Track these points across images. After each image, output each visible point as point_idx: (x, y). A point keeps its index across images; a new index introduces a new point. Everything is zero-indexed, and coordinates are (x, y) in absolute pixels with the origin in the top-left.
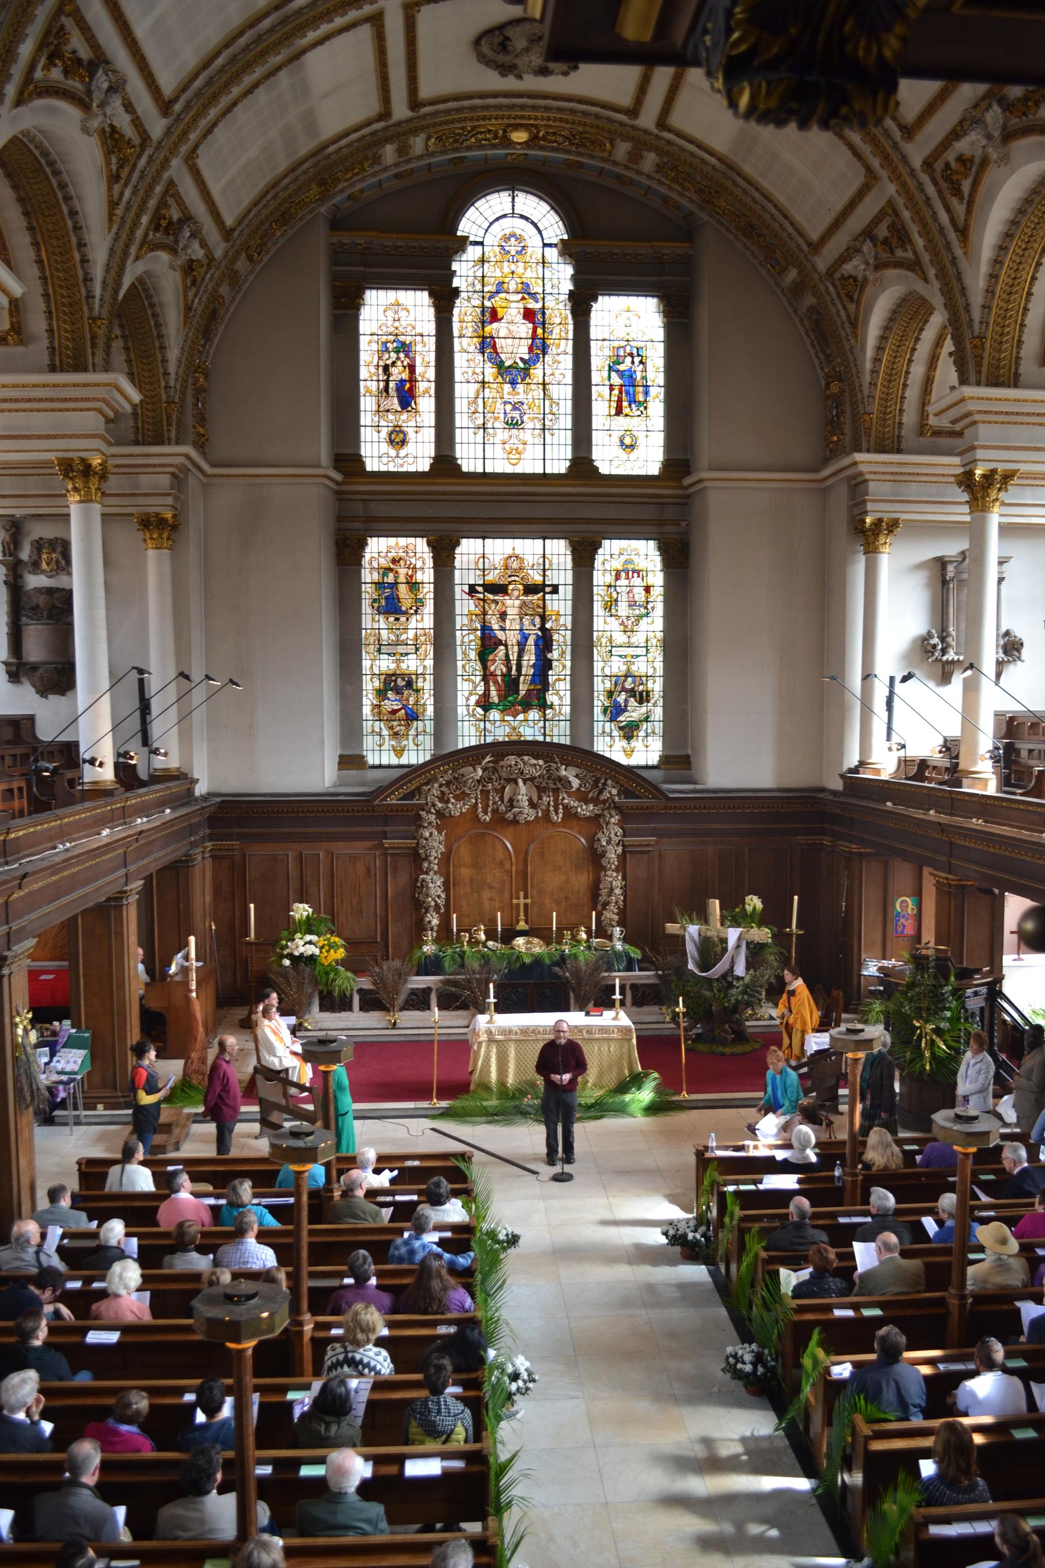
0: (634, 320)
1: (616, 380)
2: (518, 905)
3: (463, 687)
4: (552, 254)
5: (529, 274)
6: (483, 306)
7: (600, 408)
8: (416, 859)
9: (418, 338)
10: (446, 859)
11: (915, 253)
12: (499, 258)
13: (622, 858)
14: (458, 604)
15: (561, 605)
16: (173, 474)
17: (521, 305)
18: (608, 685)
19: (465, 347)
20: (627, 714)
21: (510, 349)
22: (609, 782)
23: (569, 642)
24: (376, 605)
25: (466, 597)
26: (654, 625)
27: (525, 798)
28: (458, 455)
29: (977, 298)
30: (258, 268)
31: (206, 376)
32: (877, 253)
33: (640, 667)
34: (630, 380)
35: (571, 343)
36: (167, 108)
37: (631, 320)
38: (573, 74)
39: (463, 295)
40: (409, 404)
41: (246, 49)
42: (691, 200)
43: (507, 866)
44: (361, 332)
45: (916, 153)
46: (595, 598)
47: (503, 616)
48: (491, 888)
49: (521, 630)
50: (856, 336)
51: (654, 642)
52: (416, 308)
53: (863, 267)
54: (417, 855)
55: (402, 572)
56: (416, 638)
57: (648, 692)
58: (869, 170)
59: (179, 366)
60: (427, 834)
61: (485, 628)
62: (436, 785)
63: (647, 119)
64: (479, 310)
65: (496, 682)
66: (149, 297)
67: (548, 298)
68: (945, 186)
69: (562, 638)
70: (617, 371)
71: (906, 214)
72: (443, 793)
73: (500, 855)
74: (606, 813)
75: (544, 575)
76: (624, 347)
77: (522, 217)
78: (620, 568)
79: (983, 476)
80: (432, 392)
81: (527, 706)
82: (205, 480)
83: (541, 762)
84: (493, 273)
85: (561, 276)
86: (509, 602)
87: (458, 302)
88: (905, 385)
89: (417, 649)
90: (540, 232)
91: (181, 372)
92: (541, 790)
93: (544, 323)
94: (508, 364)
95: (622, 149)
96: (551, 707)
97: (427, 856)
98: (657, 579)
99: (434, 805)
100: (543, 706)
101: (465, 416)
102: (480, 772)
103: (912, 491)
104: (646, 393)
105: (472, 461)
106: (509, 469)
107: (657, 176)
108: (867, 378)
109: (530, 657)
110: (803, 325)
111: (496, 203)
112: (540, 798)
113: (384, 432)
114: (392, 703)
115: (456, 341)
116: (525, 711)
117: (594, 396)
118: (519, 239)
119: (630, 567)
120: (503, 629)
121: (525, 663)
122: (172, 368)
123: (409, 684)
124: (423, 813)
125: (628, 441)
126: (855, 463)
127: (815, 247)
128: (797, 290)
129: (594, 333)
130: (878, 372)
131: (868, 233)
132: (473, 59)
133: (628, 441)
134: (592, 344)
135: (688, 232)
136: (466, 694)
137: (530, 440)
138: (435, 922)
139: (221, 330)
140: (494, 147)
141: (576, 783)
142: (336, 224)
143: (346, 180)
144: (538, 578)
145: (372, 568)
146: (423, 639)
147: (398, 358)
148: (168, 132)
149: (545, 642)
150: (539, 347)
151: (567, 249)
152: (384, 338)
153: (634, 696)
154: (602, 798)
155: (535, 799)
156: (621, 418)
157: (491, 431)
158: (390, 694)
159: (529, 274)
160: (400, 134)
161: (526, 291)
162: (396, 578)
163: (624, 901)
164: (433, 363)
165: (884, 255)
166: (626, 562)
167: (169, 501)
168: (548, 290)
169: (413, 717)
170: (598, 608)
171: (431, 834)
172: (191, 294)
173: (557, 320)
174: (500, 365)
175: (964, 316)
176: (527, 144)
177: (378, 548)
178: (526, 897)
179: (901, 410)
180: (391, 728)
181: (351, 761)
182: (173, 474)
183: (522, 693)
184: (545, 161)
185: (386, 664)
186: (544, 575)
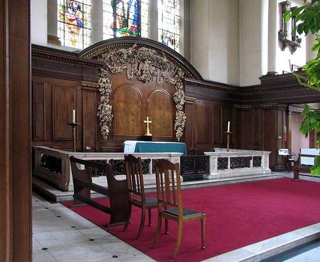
57: (175, 40)
109: (133, 10)
114: (70, 15)
123: (79, 8)
183: (129, 27)
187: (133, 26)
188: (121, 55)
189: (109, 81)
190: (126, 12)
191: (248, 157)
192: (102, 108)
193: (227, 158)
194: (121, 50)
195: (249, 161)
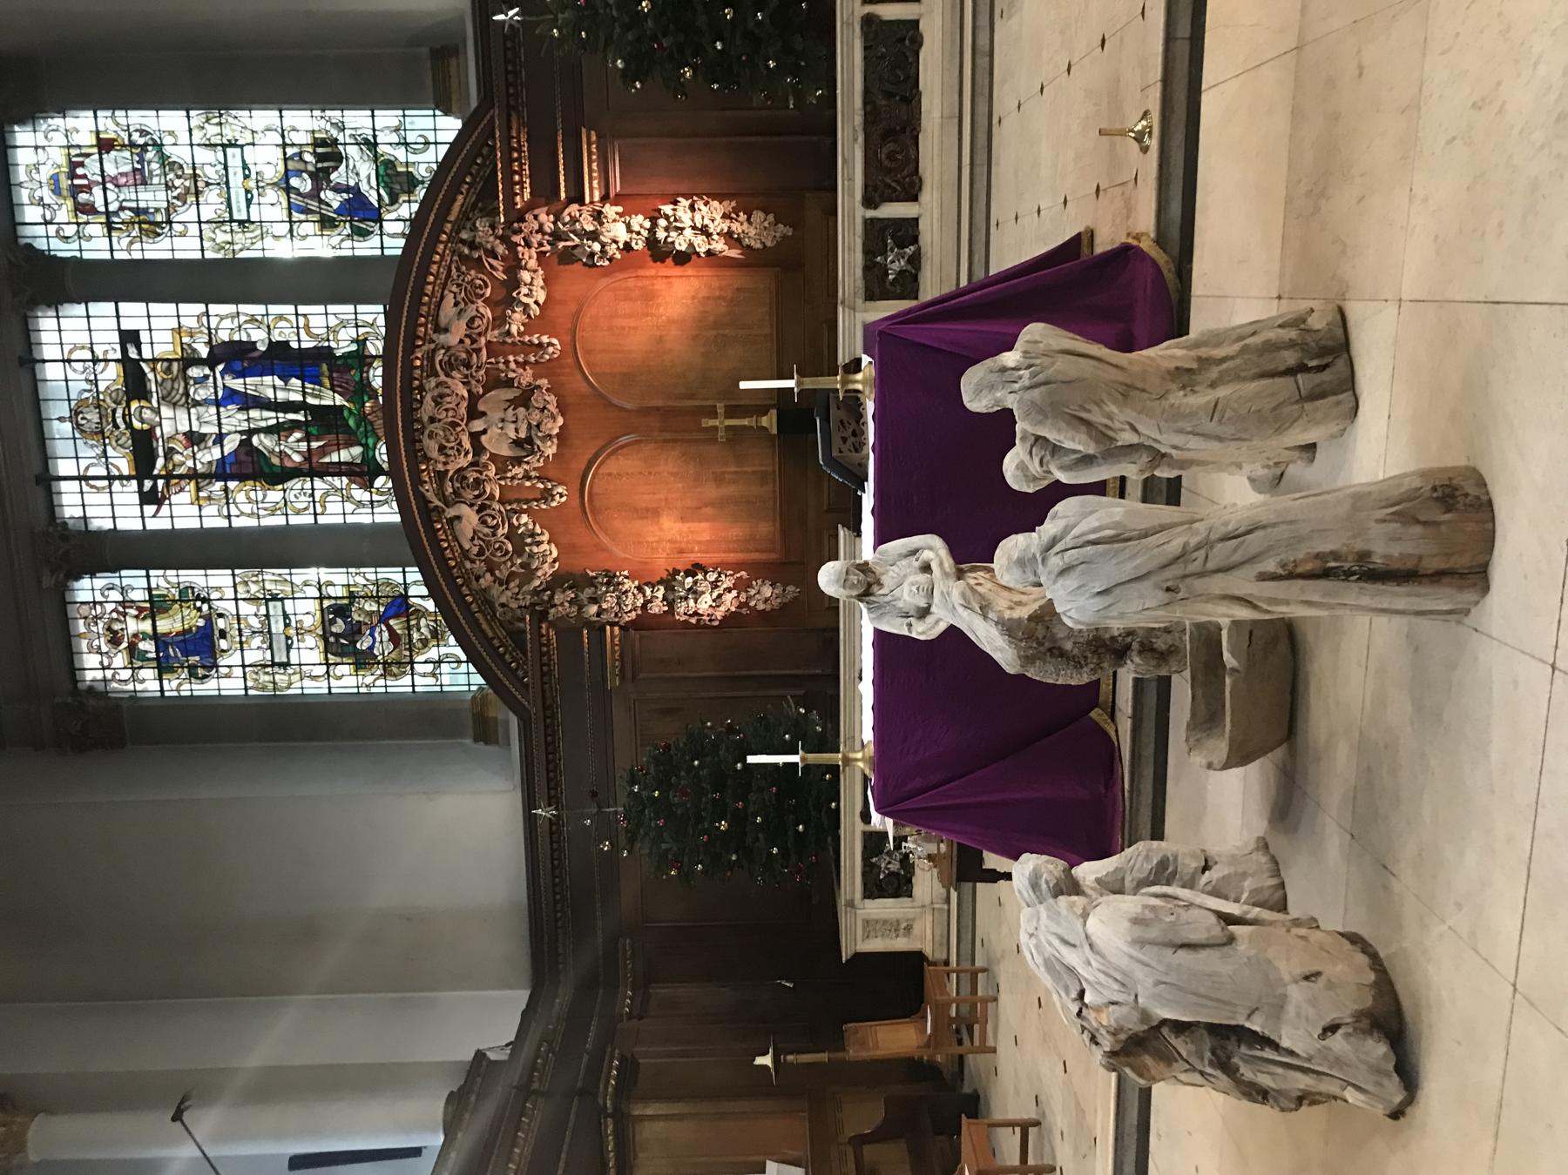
2: (728, 428)
3: (334, 514)
14: (180, 524)
15: (162, 326)
18: (309, 228)
20: (364, 187)
22: (464, 235)
24: (200, 672)
25: (165, 510)
33: (267, 160)
46: (137, 255)
47: (194, 439)
51: (212, 130)
55: (133, 626)
56: (253, 599)
57: (317, 143)
61: (223, 471)
65: (323, 451)
78: (70, 203)
89: (275, 598)
96: (361, 342)
98: (82, 126)
99: (536, 592)
100: (360, 358)
109: (266, 385)
112: (509, 383)
119: (65, 183)
120: (220, 439)
121: (281, 396)
123: (341, 611)
136: (349, 507)
138: (767, 591)
144: (111, 374)
145: (134, 678)
146: (254, 588)
149: (235, 356)
153: (327, 172)
155: (510, 394)
158: (363, 644)
162: (145, 636)
166: (57, 191)
169: (400, 605)
170: (157, 250)
178: (714, 415)
180: (425, 643)
183: (339, 400)
185: (309, 652)
186: (106, 361)
187: (327, 382)
189: (589, 591)
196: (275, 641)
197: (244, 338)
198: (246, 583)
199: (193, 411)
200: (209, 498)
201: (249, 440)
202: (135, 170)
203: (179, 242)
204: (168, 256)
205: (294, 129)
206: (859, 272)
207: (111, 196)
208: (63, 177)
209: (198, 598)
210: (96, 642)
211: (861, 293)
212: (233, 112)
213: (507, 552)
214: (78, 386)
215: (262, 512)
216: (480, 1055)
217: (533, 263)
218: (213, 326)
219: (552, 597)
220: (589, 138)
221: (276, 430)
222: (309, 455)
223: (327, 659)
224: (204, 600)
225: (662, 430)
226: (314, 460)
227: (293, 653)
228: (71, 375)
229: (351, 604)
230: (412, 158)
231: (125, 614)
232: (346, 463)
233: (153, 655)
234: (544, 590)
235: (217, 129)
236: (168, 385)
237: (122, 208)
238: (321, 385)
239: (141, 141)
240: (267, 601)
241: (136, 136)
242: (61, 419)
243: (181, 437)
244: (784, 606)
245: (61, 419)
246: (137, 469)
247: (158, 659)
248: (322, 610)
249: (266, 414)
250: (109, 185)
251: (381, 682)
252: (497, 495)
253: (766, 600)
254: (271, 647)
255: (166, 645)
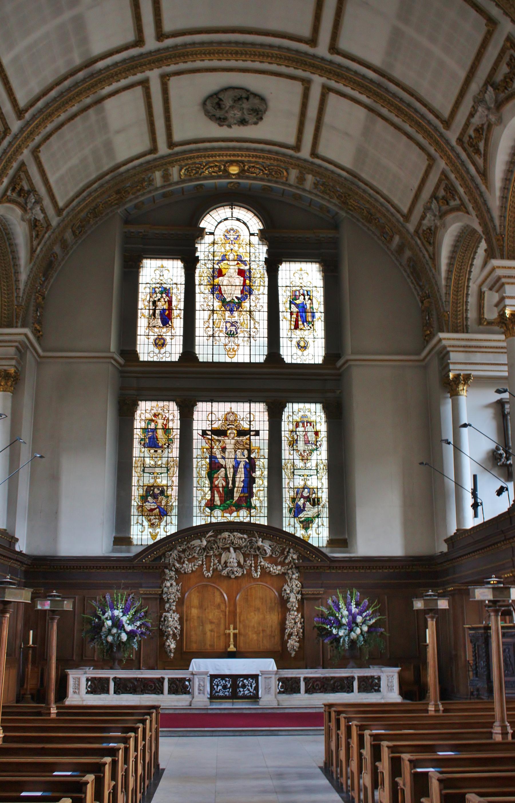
0: (305, 276)
1: (294, 309)
2: (229, 634)
4: (255, 240)
5: (241, 250)
6: (214, 268)
7: (285, 326)
8: (161, 601)
9: (174, 286)
10: (180, 602)
11: (460, 199)
12: (223, 241)
13: (301, 602)
14: (195, 441)
16: (17, 347)
17: (236, 267)
18: (292, 494)
19: (203, 290)
20: (305, 513)
21: (230, 292)
22: (291, 550)
23: (266, 466)
24: (143, 442)
26: (322, 455)
27: (235, 561)
28: (197, 352)
29: (496, 213)
30: (80, 241)
31: (44, 298)
32: (440, 207)
33: (313, 482)
34: (303, 310)
35: (266, 288)
36: (21, 113)
37: (303, 276)
38: (261, 124)
39: (202, 262)
40: (168, 323)
41: (69, 89)
42: (335, 205)
43: (223, 607)
44: (140, 282)
45: (452, 136)
46: (283, 438)
47: (224, 449)
48: (211, 623)
49: (235, 458)
50: (435, 266)
51: (322, 466)
52: (173, 271)
53: (433, 218)
54: (162, 599)
55: (160, 422)
57: (318, 499)
58: (430, 156)
59: (26, 286)
60: (168, 584)
61: (212, 457)
62: (176, 552)
63: (305, 153)
64: (211, 270)
65: (218, 492)
66: (9, 239)
67: (252, 263)
68: (470, 150)
69: (262, 463)
70: (295, 304)
71: (452, 176)
72: (180, 558)
73: (218, 600)
74: (290, 571)
75: (250, 425)
76: (299, 291)
77: (238, 220)
78: (299, 420)
79: (512, 314)
80: (182, 316)
81: (238, 507)
82: (38, 359)
83: (245, 536)
84: (219, 250)
85: (260, 251)
86: (227, 441)
87: (198, 266)
88: (467, 294)
89: (168, 470)
90: (248, 228)
91: (27, 290)
92: (245, 556)
93: (250, 277)
94: (228, 300)
95: (294, 173)
96: (255, 508)
97: (168, 601)
98: (322, 427)
99: (174, 566)
100: (250, 507)
101: (202, 330)
102: (205, 543)
103: (478, 358)
104: (313, 317)
105: (205, 356)
106: (228, 360)
107: (315, 191)
108: (443, 291)
109: (241, 475)
110: (406, 271)
111: (224, 212)
112: (245, 561)
113: (152, 338)
114: (150, 504)
115: (197, 287)
116: (237, 510)
117: (281, 318)
118: (236, 231)
119: (305, 420)
120: (224, 458)
121: (237, 480)
122: (22, 286)
123: (162, 493)
124: (167, 571)
125: (302, 344)
126: (440, 340)
127: (407, 217)
128: (401, 249)
129: (281, 282)
130: (450, 286)
131: (434, 196)
132: (202, 115)
133: (302, 344)
134: (280, 289)
135: (335, 226)
137: (241, 344)
138: (173, 646)
139: (55, 275)
140: (220, 177)
141: (269, 552)
142: (127, 221)
143: (133, 194)
144: (246, 426)
145: (142, 420)
146: (172, 463)
147: (162, 297)
148: (22, 130)
149: (251, 466)
150: (247, 291)
151: (264, 236)
152: (154, 286)
153: (310, 501)
154: (287, 561)
155: (242, 562)
156: (298, 332)
157: (217, 338)
158: (150, 499)
159: (241, 250)
160: (164, 163)
161: (239, 259)
163: (303, 633)
164: (183, 300)
165: (444, 208)
166: (302, 417)
167: (14, 362)
168: (253, 259)
169: (163, 513)
170: (285, 445)
171: (171, 585)
172: (35, 243)
173: (259, 276)
174: (224, 302)
175: (490, 225)
176: (238, 176)
177: (145, 409)
178: (235, 628)
179: (467, 310)
180: (149, 521)
181: (122, 540)
182: (17, 347)
183: (236, 499)
184: (250, 188)
185: (148, 480)
186: (250, 425)
187: (242, 495)
188: (193, 548)
189: (174, 584)
190: (230, 480)
191: (347, 678)
192: (164, 619)
193: (300, 678)
194: (193, 543)
195: (353, 684)
196: (153, 468)
197: (257, 469)
198: (173, 461)
199: (233, 450)
200: (203, 452)
201: (223, 468)
202: (309, 441)
203: (287, 452)
204: (283, 448)
205: (322, 492)
206: (286, 676)
207: (301, 433)
208: (307, 419)
209: (169, 444)
210: (155, 409)
211: (280, 676)
212: (327, 474)
213: (188, 556)
214: (241, 415)
215: (198, 469)
216: (17, 540)
217: (283, 570)
218: (261, 460)
219: (172, 571)
220: (321, 591)
221: (226, 477)
222: (217, 487)
223: (145, 486)
224: (168, 446)
225: (229, 612)
226: (216, 488)
227: (148, 475)
228: (245, 413)
229: (165, 496)
230: (314, 529)
231: (164, 420)
232: (214, 499)
233: (149, 427)
234: (175, 568)
235: (322, 468)
236: (242, 443)
237: (297, 436)
238: (241, 493)
239: (318, 444)
240: (167, 468)
241: (319, 443)
242: (231, 408)
243: (224, 445)
244: (166, 653)
245: (231, 408)
246: (214, 430)
247: (148, 429)
248: (163, 486)
249: (232, 474)
250: (304, 433)
251: (136, 504)
252: (208, 555)
253: (169, 646)
254: (150, 467)
255: (153, 432)
